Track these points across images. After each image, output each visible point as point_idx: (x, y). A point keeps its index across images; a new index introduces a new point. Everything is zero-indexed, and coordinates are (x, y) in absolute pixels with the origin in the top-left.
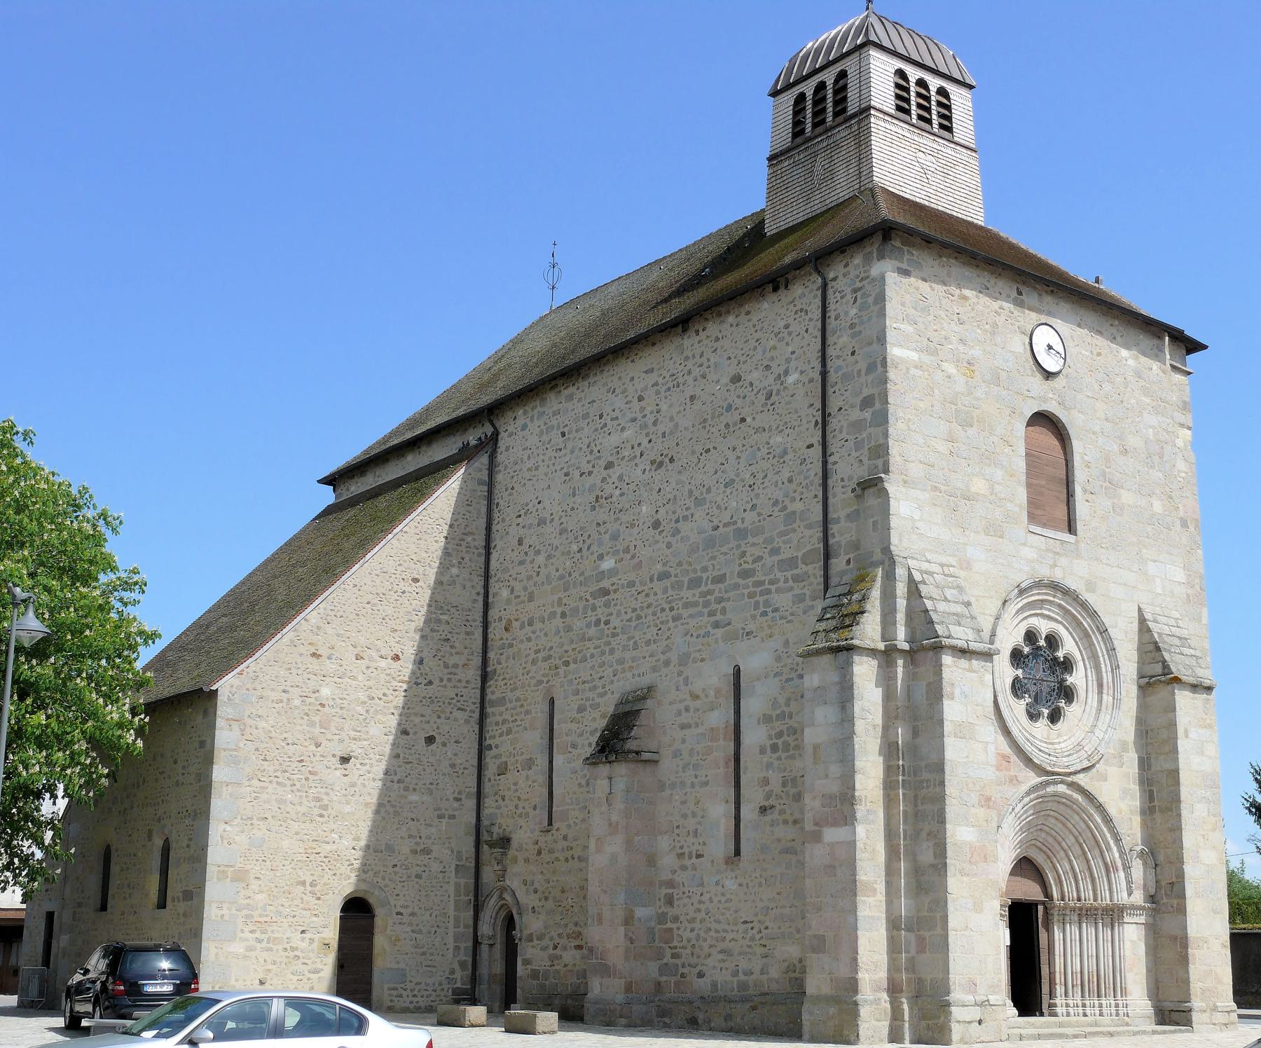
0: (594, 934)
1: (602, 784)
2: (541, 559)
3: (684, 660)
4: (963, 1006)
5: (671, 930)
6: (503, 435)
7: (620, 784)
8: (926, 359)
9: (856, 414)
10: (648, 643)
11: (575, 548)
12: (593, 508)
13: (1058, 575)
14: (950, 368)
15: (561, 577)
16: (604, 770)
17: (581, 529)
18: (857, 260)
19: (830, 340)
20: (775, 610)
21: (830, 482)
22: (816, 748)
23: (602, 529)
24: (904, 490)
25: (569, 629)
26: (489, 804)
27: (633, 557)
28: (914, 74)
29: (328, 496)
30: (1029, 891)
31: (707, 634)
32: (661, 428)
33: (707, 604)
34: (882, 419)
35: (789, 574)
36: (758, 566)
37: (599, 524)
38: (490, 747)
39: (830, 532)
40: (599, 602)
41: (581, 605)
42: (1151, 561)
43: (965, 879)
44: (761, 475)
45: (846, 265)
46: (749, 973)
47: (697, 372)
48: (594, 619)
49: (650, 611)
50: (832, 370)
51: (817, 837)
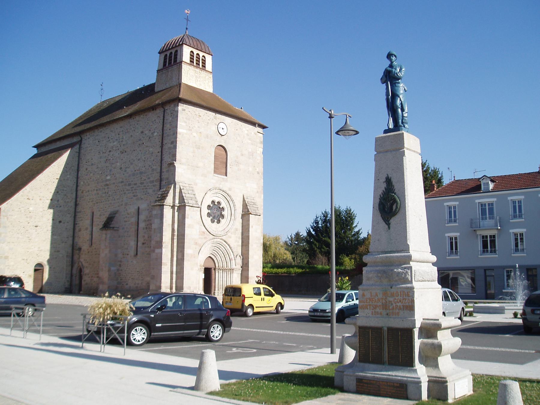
0: (101, 274)
1: (104, 236)
2: (92, 175)
3: (126, 204)
5: (120, 273)
6: (83, 140)
7: (108, 236)
9: (169, 145)
10: (118, 199)
11: (100, 172)
12: (106, 162)
13: (221, 187)
14: (195, 134)
15: (97, 180)
16: (104, 232)
17: (102, 167)
18: (172, 106)
19: (165, 125)
20: (148, 193)
21: (163, 162)
22: (155, 229)
23: (107, 168)
25: (98, 194)
26: (76, 239)
27: (115, 176)
28: (196, 52)
29: (35, 151)
30: (210, 265)
31: (132, 198)
32: (124, 143)
33: (132, 190)
34: (175, 147)
35: (152, 184)
36: (145, 182)
37: (107, 167)
38: (77, 224)
39: (162, 175)
40: (106, 187)
41: (102, 188)
44: (147, 158)
45: (170, 106)
46: (138, 284)
47: (133, 129)
48: (104, 192)
49: (118, 191)
50: (165, 134)
51: (154, 251)
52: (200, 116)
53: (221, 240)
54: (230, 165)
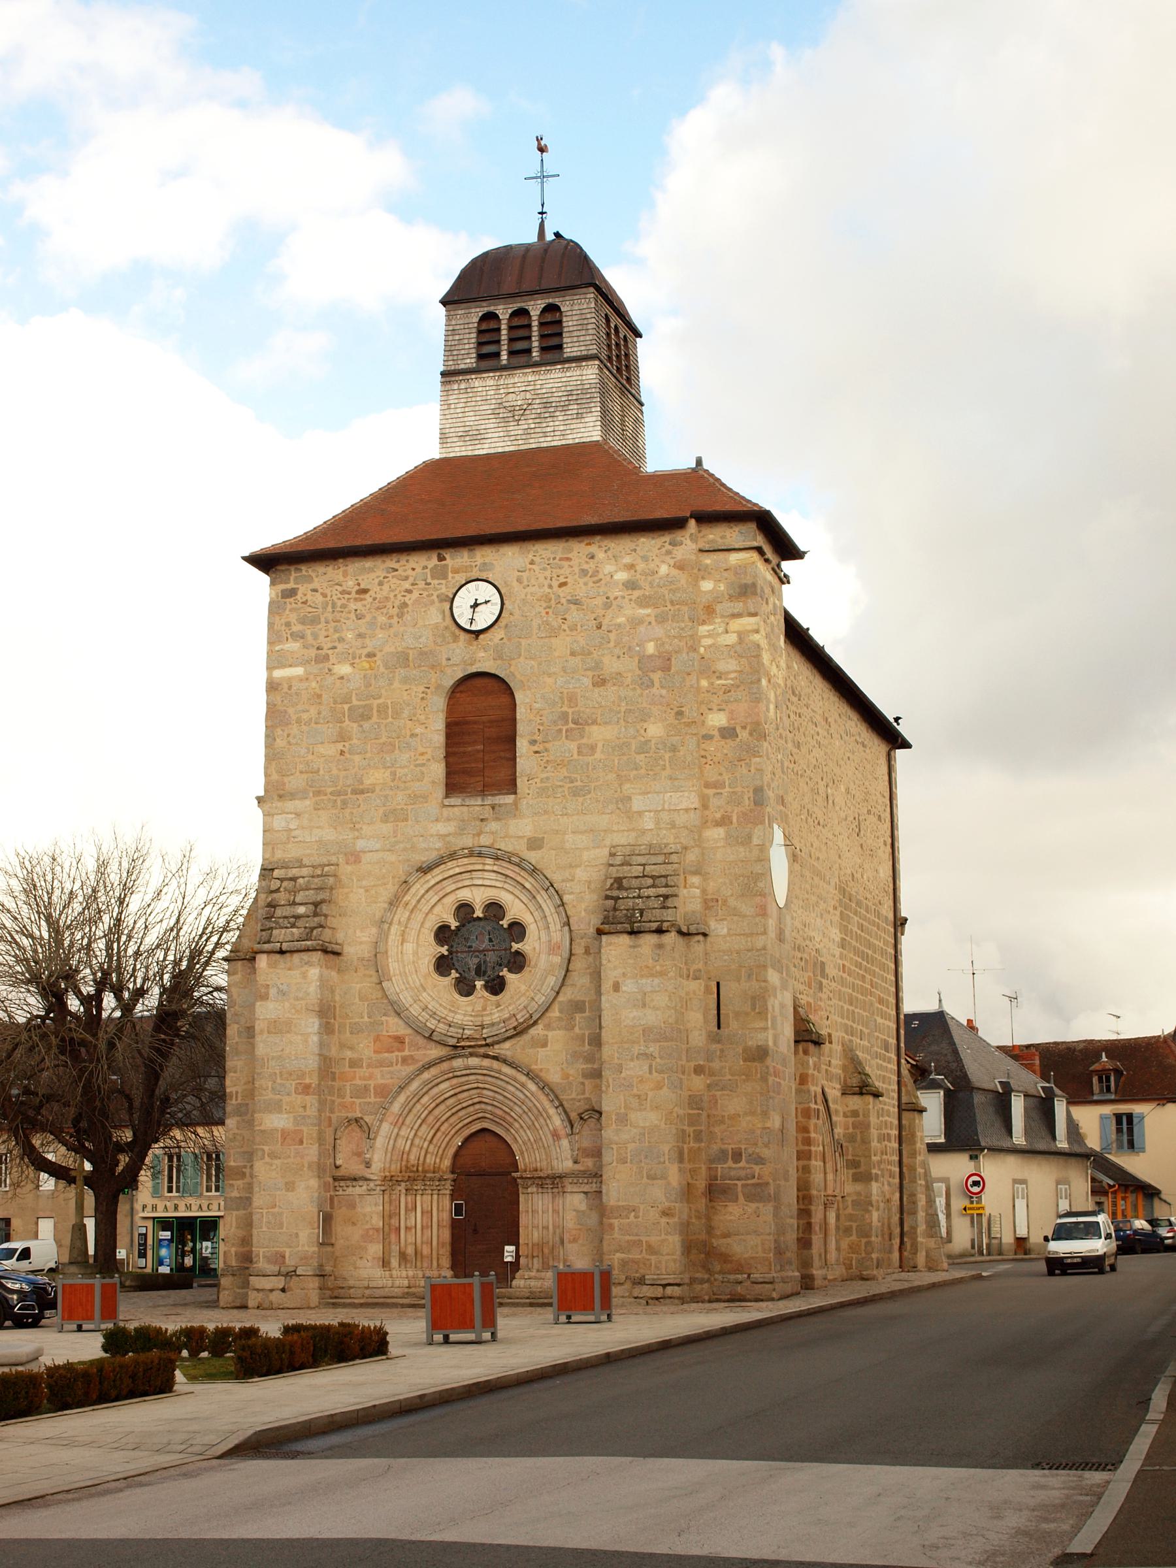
4: (264, 1276)
8: (315, 668)
14: (345, 669)
24: (279, 804)
42: (640, 794)
43: (277, 1162)
52: (365, 591)
53: (486, 1062)
54: (533, 742)
